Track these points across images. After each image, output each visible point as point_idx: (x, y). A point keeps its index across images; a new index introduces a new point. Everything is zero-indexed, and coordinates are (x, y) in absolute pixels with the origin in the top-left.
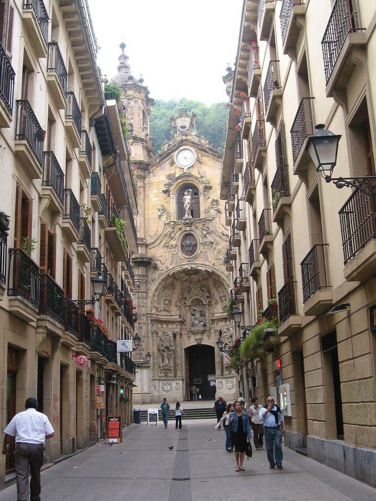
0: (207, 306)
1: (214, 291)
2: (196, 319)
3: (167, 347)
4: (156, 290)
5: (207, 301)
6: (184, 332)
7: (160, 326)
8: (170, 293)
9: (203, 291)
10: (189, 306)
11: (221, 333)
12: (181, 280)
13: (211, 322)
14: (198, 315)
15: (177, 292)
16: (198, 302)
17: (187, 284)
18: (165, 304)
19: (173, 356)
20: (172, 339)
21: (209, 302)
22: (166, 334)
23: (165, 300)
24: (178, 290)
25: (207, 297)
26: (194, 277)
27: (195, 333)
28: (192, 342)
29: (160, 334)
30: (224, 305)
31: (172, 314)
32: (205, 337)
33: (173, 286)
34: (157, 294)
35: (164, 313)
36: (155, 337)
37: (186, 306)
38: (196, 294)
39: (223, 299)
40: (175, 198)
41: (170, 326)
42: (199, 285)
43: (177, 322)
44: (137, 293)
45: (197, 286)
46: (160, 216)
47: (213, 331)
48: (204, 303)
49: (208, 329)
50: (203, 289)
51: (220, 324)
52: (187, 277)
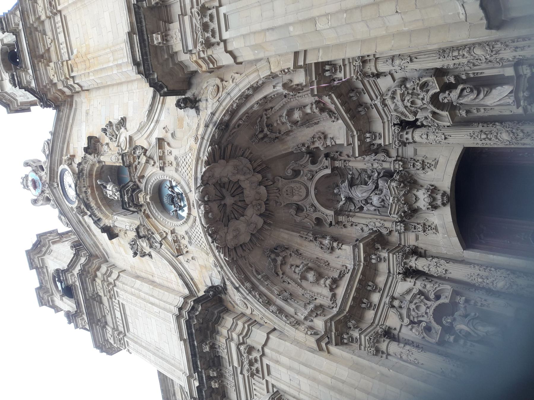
0: (337, 164)
1: (291, 144)
2: (367, 201)
3: (439, 313)
4: (268, 303)
5: (326, 162)
6: (411, 239)
7: (370, 314)
8: (298, 262)
9: (296, 173)
10: (338, 213)
11: (405, 125)
12: (260, 231)
13: (381, 156)
14: (359, 193)
15: (299, 240)
16: (327, 191)
17: (282, 214)
18: (317, 281)
19: (476, 296)
20: (419, 284)
21: (327, 156)
22: (396, 303)
23: (304, 278)
24: (293, 239)
25: (314, 162)
26: (249, 193)
27: (409, 209)
28: (443, 218)
29: (393, 321)
30: (316, 111)
31: (350, 267)
32: (427, 177)
33: (280, 251)
34: (280, 302)
35: (341, 291)
36: (394, 347)
37: (338, 223)
38: (304, 191)
39: (297, 115)
40: (116, 217)
41: (381, 280)
42: (281, 183)
43: (368, 258)
44: (265, 361)
45: (284, 190)
46: (143, 255)
47: (409, 151)
48: (328, 171)
49: (399, 166)
50: (289, 172)
51: (378, 127)
52: (249, 212)
